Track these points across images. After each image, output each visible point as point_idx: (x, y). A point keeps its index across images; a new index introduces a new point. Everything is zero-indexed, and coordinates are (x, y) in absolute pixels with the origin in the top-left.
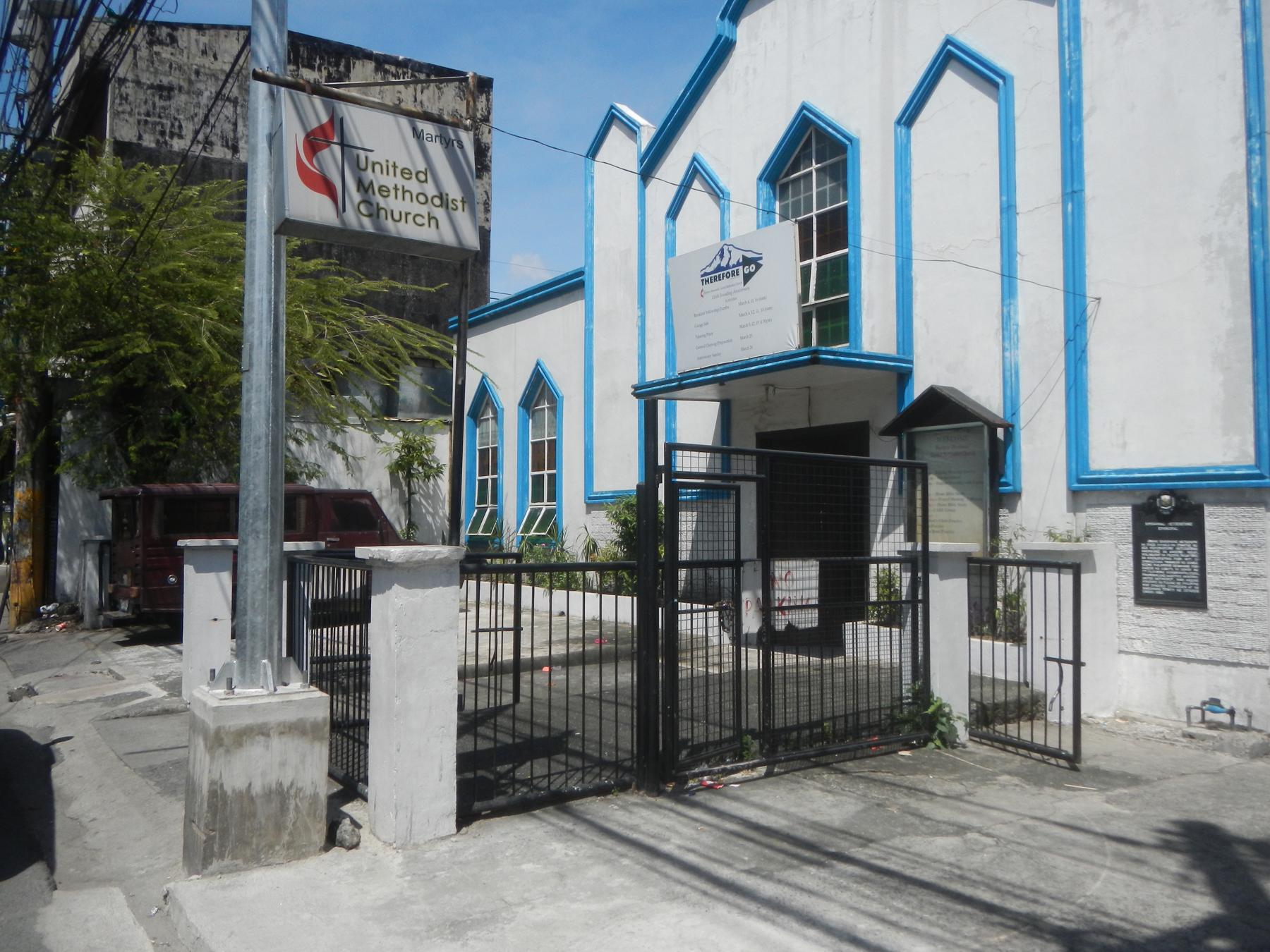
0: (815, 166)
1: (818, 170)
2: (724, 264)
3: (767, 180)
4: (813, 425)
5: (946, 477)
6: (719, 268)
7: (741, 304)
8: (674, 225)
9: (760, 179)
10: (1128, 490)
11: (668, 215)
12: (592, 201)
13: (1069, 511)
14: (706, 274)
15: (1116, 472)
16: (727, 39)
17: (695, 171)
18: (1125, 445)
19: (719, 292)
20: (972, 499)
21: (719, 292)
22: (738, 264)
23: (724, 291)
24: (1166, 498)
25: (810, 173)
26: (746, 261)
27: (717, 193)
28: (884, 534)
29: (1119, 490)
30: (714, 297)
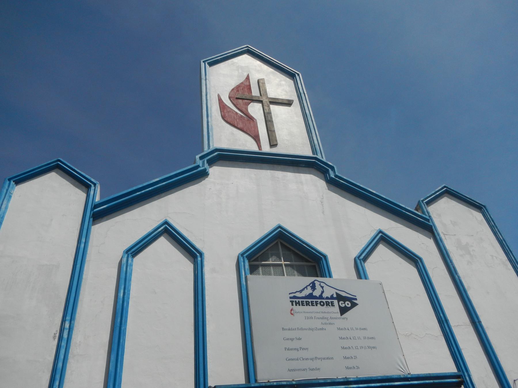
0: (283, 262)
2: (317, 293)
3: (249, 258)
6: (311, 296)
7: (339, 329)
8: (132, 261)
9: (242, 254)
11: (127, 251)
12: (4, 213)
14: (295, 297)
16: (205, 170)
17: (168, 231)
19: (313, 315)
22: (332, 297)
23: (321, 315)
25: (281, 265)
26: (340, 298)
30: (308, 318)
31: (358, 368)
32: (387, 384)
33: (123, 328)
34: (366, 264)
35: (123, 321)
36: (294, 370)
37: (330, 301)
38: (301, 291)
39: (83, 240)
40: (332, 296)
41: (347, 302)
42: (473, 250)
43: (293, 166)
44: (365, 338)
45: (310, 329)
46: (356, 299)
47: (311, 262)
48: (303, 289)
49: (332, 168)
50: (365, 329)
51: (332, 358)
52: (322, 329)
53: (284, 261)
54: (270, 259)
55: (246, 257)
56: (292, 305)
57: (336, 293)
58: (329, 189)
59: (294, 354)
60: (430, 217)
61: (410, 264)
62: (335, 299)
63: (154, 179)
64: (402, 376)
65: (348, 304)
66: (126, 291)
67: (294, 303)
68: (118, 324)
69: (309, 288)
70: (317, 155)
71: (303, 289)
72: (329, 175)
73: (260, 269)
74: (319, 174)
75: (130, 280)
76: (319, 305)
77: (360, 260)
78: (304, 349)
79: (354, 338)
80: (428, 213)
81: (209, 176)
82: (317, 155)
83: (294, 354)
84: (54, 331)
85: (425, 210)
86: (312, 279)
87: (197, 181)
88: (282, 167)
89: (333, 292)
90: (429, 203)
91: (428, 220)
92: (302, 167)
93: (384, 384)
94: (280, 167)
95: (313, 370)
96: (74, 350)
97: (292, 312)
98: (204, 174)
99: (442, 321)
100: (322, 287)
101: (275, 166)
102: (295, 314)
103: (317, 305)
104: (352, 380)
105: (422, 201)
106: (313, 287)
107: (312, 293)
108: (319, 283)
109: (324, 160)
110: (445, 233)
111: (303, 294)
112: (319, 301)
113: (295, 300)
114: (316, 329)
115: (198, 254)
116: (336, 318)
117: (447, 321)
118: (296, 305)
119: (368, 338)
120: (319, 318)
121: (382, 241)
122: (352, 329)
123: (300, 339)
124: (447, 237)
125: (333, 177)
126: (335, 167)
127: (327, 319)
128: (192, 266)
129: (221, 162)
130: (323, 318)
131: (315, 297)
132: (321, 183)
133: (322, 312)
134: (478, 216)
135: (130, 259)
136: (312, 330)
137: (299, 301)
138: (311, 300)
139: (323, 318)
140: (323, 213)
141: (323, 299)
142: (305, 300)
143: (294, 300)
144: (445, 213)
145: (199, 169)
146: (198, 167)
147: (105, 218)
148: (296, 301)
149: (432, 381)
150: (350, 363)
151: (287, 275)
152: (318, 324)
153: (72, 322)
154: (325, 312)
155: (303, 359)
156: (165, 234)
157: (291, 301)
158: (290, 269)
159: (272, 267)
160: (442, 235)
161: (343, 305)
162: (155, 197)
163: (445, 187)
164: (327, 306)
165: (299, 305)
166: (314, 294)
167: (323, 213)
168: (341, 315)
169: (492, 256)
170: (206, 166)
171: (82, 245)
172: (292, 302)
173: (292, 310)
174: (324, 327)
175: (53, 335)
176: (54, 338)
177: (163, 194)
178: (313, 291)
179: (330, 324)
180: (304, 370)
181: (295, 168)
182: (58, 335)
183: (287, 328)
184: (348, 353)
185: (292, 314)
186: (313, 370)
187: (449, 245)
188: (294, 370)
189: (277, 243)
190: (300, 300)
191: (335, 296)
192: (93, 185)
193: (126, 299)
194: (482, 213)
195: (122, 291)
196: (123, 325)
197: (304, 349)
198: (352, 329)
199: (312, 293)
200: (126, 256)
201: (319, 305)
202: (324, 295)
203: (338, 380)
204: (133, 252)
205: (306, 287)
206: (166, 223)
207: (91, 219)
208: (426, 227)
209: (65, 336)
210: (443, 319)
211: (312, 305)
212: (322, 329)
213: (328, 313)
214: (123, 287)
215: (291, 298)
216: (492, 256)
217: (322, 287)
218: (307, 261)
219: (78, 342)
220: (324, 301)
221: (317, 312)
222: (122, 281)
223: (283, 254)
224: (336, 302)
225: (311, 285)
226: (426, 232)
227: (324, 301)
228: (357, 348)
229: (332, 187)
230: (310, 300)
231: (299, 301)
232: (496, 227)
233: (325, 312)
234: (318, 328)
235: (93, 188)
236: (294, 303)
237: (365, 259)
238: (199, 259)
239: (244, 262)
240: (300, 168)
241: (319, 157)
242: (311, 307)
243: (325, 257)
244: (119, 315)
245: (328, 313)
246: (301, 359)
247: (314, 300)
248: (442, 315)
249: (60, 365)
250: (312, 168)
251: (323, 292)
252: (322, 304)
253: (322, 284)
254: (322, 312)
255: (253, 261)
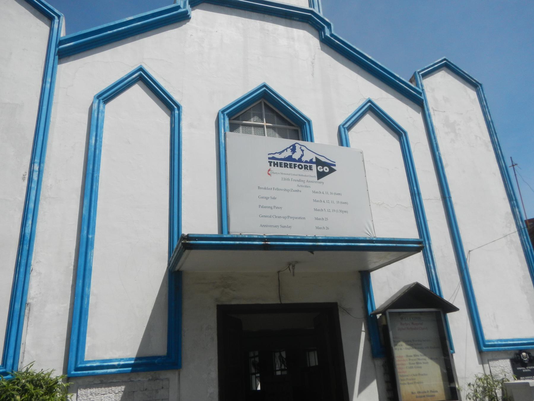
0: (265, 124)
1: (267, 127)
2: (296, 156)
3: (230, 115)
4: (284, 302)
5: (412, 343)
6: (290, 158)
7: (314, 192)
8: (104, 107)
9: (223, 112)
10: (505, 351)
11: (99, 96)
13: (480, 364)
14: (273, 158)
15: (498, 340)
16: (186, 12)
17: (142, 78)
18: (497, 327)
19: (290, 177)
20: (431, 359)
21: (290, 177)
22: (311, 162)
23: (298, 178)
24: (524, 354)
25: (262, 126)
26: (319, 162)
27: (169, 104)
28: (360, 390)
29: (498, 351)
30: (285, 179)
31: (328, 228)
32: (353, 244)
33: (95, 175)
34: (349, 133)
35: (96, 168)
36: (267, 226)
37: (308, 165)
38: (280, 153)
39: (49, 80)
40: (311, 160)
41: (325, 168)
42: (459, 129)
43: (286, 18)
44: (338, 202)
45: (285, 190)
46: (335, 165)
47: (293, 124)
48: (283, 151)
49: (329, 25)
50: (339, 194)
51: (304, 218)
52: (298, 191)
53: (266, 123)
54: (252, 119)
55: (227, 114)
56: (271, 165)
57: (316, 158)
58: (322, 49)
59: (268, 212)
60: (423, 90)
61: (394, 136)
62: (313, 163)
63: (127, 17)
64: (368, 239)
65: (326, 169)
66: (98, 138)
67: (272, 164)
68: (90, 171)
69: (289, 150)
70: (314, 8)
71: (283, 151)
72: (324, 33)
73: (241, 128)
74: (313, 30)
75: (102, 127)
76: (297, 168)
77: (344, 128)
78: (277, 208)
79: (328, 202)
80: (422, 86)
81: (191, 20)
82: (314, 8)
83: (268, 212)
84: (23, 173)
85: (420, 83)
86: (293, 142)
87: (177, 24)
88: (274, 18)
89: (313, 157)
90: (425, 76)
91: (420, 94)
92: (295, 20)
93: (350, 244)
94: (271, 18)
95: (284, 227)
96: (44, 192)
97: (270, 172)
98: (184, 17)
99: (415, 194)
100: (303, 151)
101: (266, 16)
102: (272, 174)
103: (295, 168)
104: (320, 238)
105: (419, 72)
106: (294, 150)
107: (291, 156)
108: (300, 146)
109: (321, 15)
110: (435, 109)
111: (282, 156)
112: (298, 164)
113: (274, 161)
114: (292, 190)
115: (175, 107)
116: (312, 182)
117: (419, 194)
118: (274, 166)
119: (341, 203)
120: (295, 181)
121: (369, 111)
122: (327, 193)
123: (274, 198)
124: (436, 112)
125: (329, 35)
126: (332, 24)
127: (303, 181)
128: (169, 119)
129: (205, 5)
130: (299, 181)
131: (294, 160)
132: (314, 42)
133: (300, 175)
134: (472, 94)
135: (101, 105)
136: (288, 191)
137: (277, 163)
138: (289, 162)
139: (299, 181)
140: (313, 75)
141: (302, 162)
142: (283, 162)
143: (273, 161)
144: (440, 88)
145: (180, 11)
146: (178, 7)
147: (72, 57)
148: (274, 162)
149: (395, 245)
150: (321, 224)
151: (268, 136)
152: (294, 185)
153: (42, 165)
154: (302, 175)
155: (276, 217)
156: (140, 82)
157: (269, 162)
158: (271, 131)
159: (253, 128)
160: (431, 111)
161: (321, 170)
162: (129, 39)
163: (445, 59)
164: (305, 169)
165: (277, 166)
166: (294, 157)
167: (313, 75)
168: (318, 179)
169: (476, 136)
170: (188, 7)
171: (48, 85)
172: (270, 163)
173: (269, 170)
174: (300, 189)
175: (22, 176)
176: (24, 179)
177: (138, 36)
178: (293, 153)
179: (306, 186)
180: (276, 226)
181: (288, 21)
182: (27, 176)
183: (263, 187)
184: (319, 215)
185: (269, 174)
186: (284, 227)
187: (436, 121)
188: (267, 226)
189: (261, 103)
190: (279, 161)
191: (314, 160)
192: (56, 17)
193: (98, 146)
194: (476, 92)
195: (94, 138)
196: (95, 172)
197: (277, 208)
198: (327, 193)
199: (291, 156)
200: (97, 101)
201: (297, 168)
202: (304, 159)
203: (307, 238)
204: (105, 98)
205: (286, 149)
206: (141, 69)
207: (57, 57)
208: (417, 100)
209: (35, 177)
210: (416, 192)
211: (291, 167)
212: (298, 191)
213: (305, 176)
214: (94, 134)
215: (269, 158)
216: (476, 136)
217: (303, 151)
218: (290, 124)
219: (49, 185)
220: (303, 164)
221: (295, 175)
222: (94, 128)
223: (266, 115)
224: (314, 166)
225: (292, 148)
226: (416, 106)
227: (303, 164)
228: (329, 211)
229: (326, 48)
230: (288, 163)
231: (277, 163)
232: (488, 107)
233: (302, 175)
234: (294, 189)
235: (56, 20)
236: (272, 164)
237: (349, 128)
238: (177, 112)
239: (224, 119)
240: (294, 22)
241: (316, 11)
242: (289, 169)
243: (309, 122)
244: (91, 162)
245: (305, 176)
246: (274, 217)
247: (293, 163)
248: (415, 188)
249: (32, 205)
250: (307, 22)
251: (302, 155)
252: (300, 167)
253: (303, 148)
254: (300, 175)
255: (233, 120)
